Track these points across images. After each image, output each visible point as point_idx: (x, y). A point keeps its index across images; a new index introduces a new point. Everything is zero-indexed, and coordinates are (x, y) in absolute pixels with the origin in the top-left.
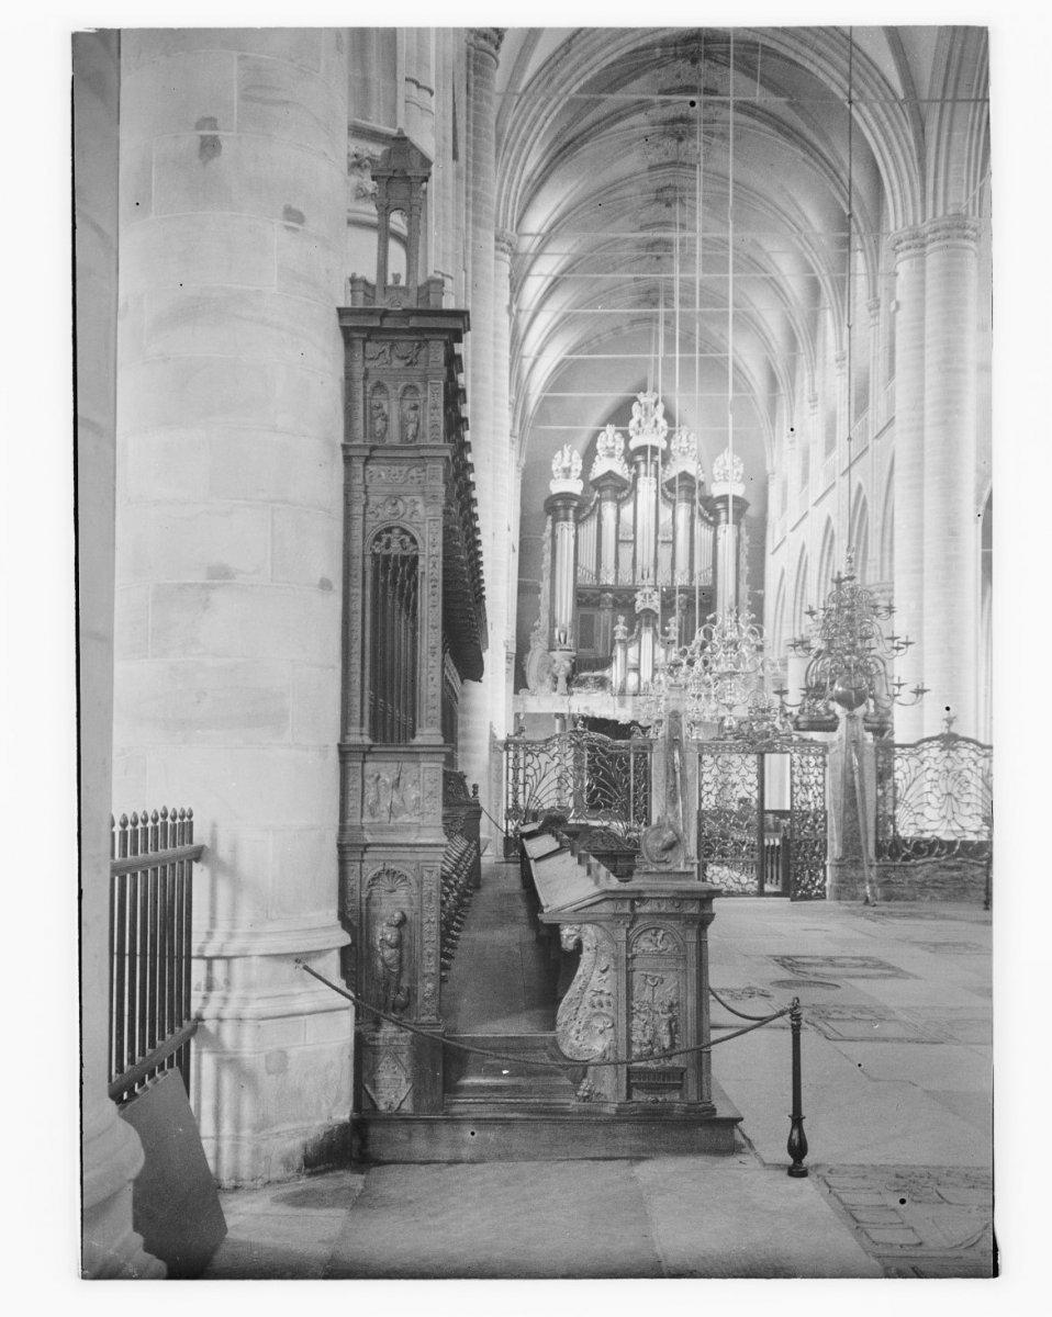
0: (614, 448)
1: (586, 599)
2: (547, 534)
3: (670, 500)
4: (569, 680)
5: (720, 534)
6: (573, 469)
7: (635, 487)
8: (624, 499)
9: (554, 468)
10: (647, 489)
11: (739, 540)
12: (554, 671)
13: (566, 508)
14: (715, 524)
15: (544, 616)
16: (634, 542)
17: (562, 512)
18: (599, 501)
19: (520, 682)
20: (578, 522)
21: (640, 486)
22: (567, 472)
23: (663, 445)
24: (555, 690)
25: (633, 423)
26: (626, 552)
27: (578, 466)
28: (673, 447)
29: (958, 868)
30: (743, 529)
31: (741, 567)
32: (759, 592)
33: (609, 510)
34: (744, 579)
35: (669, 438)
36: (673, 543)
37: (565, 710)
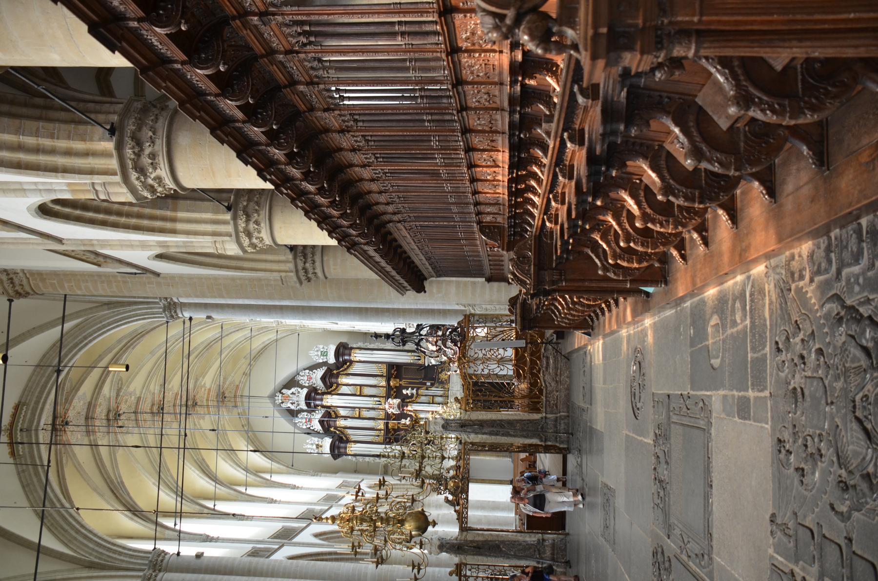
1: (391, 436)
3: (337, 387)
5: (357, 359)
7: (329, 407)
8: (335, 413)
10: (331, 400)
11: (360, 349)
13: (339, 448)
14: (351, 362)
16: (359, 408)
17: (342, 450)
18: (336, 428)
20: (348, 441)
21: (329, 404)
22: (318, 446)
23: (305, 391)
25: (293, 407)
26: (365, 414)
27: (316, 440)
29: (548, 358)
30: (355, 346)
33: (341, 423)
35: (302, 387)
36: (361, 386)
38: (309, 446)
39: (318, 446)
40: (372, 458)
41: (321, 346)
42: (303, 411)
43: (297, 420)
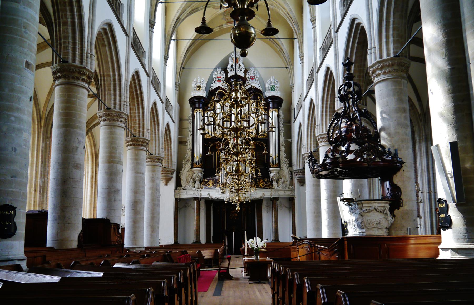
0: (221, 77)
2: (191, 116)
4: (201, 182)
6: (202, 86)
9: (193, 85)
11: (279, 116)
12: (194, 177)
13: (199, 103)
14: (267, 110)
15: (189, 153)
17: (197, 105)
19: (178, 184)
22: (199, 87)
24: (194, 187)
25: (229, 66)
27: (204, 85)
28: (247, 76)
30: (281, 112)
31: (280, 128)
32: (289, 140)
34: (282, 134)
35: (245, 72)
37: (199, 196)
38: (199, 80)
39: (199, 87)
40: (191, 129)
41: (278, 85)
42: (226, 75)
43: (219, 70)
